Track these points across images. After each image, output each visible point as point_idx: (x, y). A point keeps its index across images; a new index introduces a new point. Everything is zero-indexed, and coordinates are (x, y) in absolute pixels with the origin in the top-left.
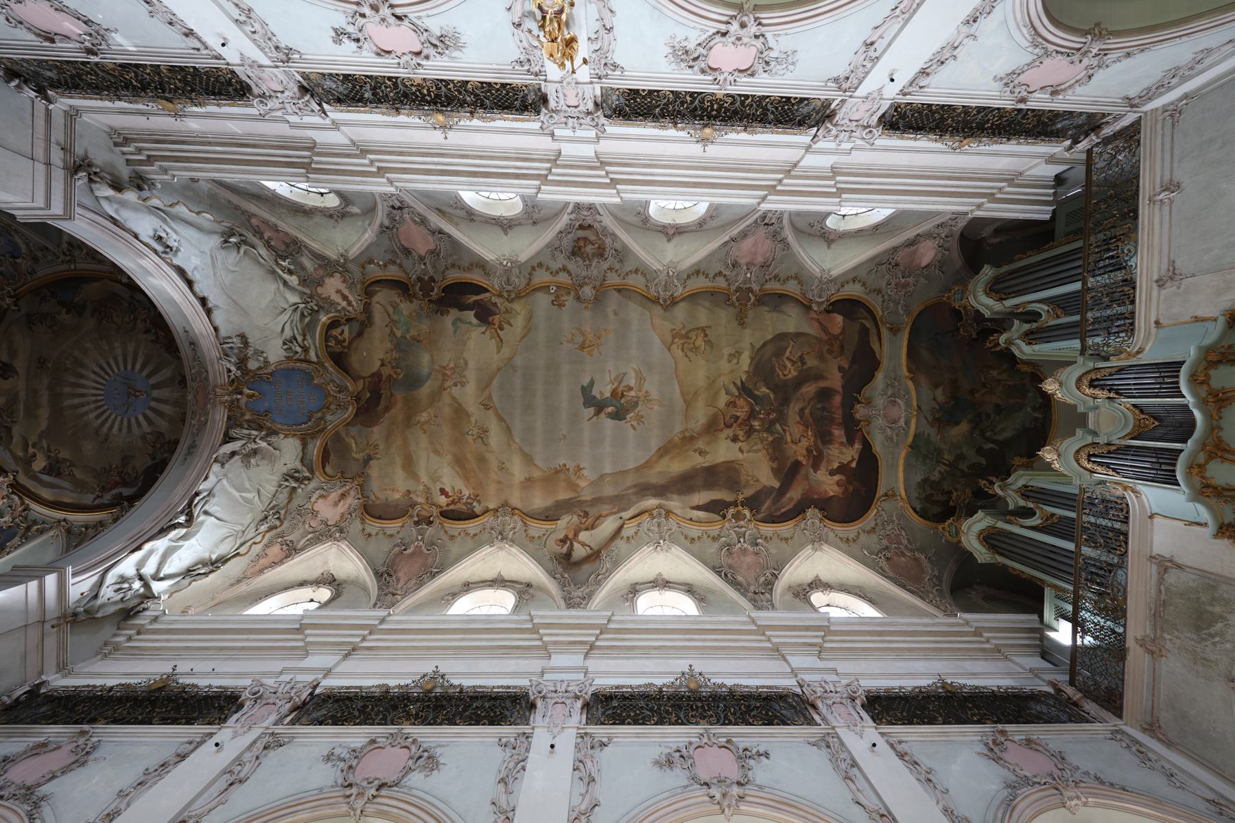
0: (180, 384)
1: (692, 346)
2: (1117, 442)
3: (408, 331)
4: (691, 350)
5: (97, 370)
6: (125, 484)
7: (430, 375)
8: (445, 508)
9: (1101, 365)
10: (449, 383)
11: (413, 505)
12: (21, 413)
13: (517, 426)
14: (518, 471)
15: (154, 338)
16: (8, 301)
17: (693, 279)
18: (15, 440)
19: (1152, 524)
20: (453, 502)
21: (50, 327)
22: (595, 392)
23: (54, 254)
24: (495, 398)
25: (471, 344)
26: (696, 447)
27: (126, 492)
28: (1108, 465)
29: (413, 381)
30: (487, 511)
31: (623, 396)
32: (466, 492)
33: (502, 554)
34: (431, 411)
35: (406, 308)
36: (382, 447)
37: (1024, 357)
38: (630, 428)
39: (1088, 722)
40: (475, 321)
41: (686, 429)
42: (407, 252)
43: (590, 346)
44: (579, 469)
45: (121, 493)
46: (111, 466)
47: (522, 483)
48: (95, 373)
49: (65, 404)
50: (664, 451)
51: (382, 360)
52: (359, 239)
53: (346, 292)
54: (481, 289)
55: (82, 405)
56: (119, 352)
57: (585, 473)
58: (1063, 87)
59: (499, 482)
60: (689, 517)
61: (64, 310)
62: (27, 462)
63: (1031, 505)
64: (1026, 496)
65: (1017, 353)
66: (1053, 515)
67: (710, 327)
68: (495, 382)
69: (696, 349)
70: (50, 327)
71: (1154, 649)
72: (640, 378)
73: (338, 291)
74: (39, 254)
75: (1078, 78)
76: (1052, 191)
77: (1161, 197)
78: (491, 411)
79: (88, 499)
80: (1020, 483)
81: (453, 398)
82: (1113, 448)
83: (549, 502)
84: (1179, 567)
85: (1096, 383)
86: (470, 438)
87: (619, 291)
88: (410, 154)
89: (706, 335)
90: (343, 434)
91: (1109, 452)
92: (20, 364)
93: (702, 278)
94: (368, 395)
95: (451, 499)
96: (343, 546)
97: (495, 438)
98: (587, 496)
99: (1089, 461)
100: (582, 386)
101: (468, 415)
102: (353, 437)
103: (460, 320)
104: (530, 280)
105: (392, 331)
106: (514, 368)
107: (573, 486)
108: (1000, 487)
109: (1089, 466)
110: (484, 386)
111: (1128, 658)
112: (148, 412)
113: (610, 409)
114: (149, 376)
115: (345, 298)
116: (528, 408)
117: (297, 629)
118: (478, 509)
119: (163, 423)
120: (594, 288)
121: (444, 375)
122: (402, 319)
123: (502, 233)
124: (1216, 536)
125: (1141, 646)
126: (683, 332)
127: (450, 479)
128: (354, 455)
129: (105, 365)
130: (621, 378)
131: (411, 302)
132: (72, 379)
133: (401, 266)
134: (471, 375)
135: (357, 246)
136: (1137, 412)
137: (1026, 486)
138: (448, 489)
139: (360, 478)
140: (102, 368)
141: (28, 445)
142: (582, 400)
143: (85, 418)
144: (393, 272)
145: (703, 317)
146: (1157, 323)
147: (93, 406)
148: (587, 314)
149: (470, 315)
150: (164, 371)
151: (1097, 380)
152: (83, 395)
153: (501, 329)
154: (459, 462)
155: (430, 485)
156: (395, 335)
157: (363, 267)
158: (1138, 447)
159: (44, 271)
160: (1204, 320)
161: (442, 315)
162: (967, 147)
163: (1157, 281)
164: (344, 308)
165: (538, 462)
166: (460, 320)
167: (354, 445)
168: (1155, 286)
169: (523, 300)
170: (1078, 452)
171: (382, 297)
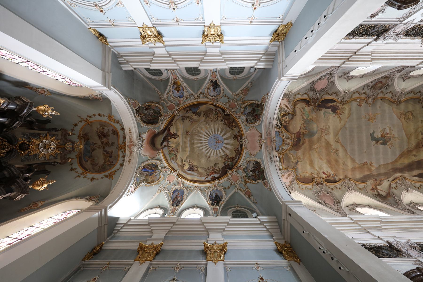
0: (233, 138)
1: (408, 118)
3: (308, 117)
4: (407, 119)
5: (206, 134)
6: (216, 173)
7: (317, 132)
8: (325, 179)
10: (324, 134)
11: (315, 178)
12: (180, 150)
13: (349, 149)
14: (350, 165)
15: (224, 123)
16: (177, 112)
17: (409, 94)
18: (178, 159)
20: (328, 177)
21: (190, 121)
22: (375, 135)
23: (194, 96)
24: (340, 139)
25: (331, 120)
26: (413, 154)
27: (216, 176)
29: (311, 134)
30: (340, 180)
31: (385, 136)
32: (332, 173)
33: (352, 195)
34: (318, 144)
35: (308, 109)
36: (302, 157)
38: (389, 148)
40: (331, 112)
41: (409, 148)
42: (314, 90)
43: (372, 119)
44: (371, 163)
45: (214, 176)
46: (210, 167)
47: (351, 169)
48: (205, 135)
49: (195, 146)
50: (402, 156)
51: (300, 127)
52: (299, 86)
53: (287, 105)
54: (333, 101)
55: (201, 146)
56: (213, 128)
57: (374, 164)
59: (343, 169)
60: (413, 179)
61: (194, 115)
62: (183, 166)
67: (413, 111)
68: (340, 133)
69: (409, 119)
70: (190, 121)
72: (391, 130)
73: (284, 104)
74: (189, 96)
78: (339, 144)
79: (203, 179)
81: (326, 140)
83: (362, 176)
86: (332, 153)
87: (381, 99)
88: (386, 53)
89: (412, 114)
90: (288, 154)
92: (180, 133)
93: (412, 94)
94: (296, 139)
95: (327, 175)
96: (296, 193)
97: (341, 153)
98: (375, 173)
100: (371, 134)
101: (331, 145)
102: (292, 155)
103: (326, 112)
104: (351, 97)
105: (303, 117)
106: (346, 128)
107: (370, 170)
110: (336, 135)
112: (223, 148)
113: (381, 141)
114: (223, 136)
115: (287, 107)
116: (352, 142)
117: (354, 222)
118: (337, 179)
119: (228, 151)
120: (373, 99)
121: (322, 131)
122: (306, 113)
123: (347, 81)
126: (404, 113)
127: (326, 168)
128: (292, 161)
129: (208, 133)
130: (384, 130)
131: (309, 107)
132: (197, 138)
133: (308, 95)
134: (331, 131)
135: (297, 89)
138: (325, 172)
139: (295, 168)
140: (207, 133)
141: (183, 161)
142: (371, 139)
143: (202, 151)
144: (305, 97)
145: (410, 108)
147: (204, 147)
148: (370, 108)
149: (329, 110)
150: (228, 134)
152: (201, 143)
153: (341, 114)
154: (329, 162)
155: (319, 171)
156: (304, 119)
157: (295, 96)
159: (189, 102)
161: (320, 110)
164: (287, 110)
165: (357, 161)
166: (326, 112)
167: (292, 157)
169: (348, 104)
171: (299, 105)
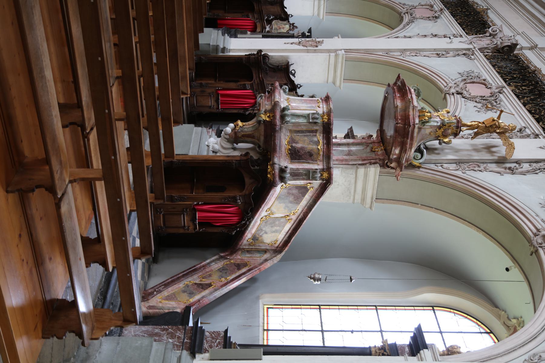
162: (484, 7)
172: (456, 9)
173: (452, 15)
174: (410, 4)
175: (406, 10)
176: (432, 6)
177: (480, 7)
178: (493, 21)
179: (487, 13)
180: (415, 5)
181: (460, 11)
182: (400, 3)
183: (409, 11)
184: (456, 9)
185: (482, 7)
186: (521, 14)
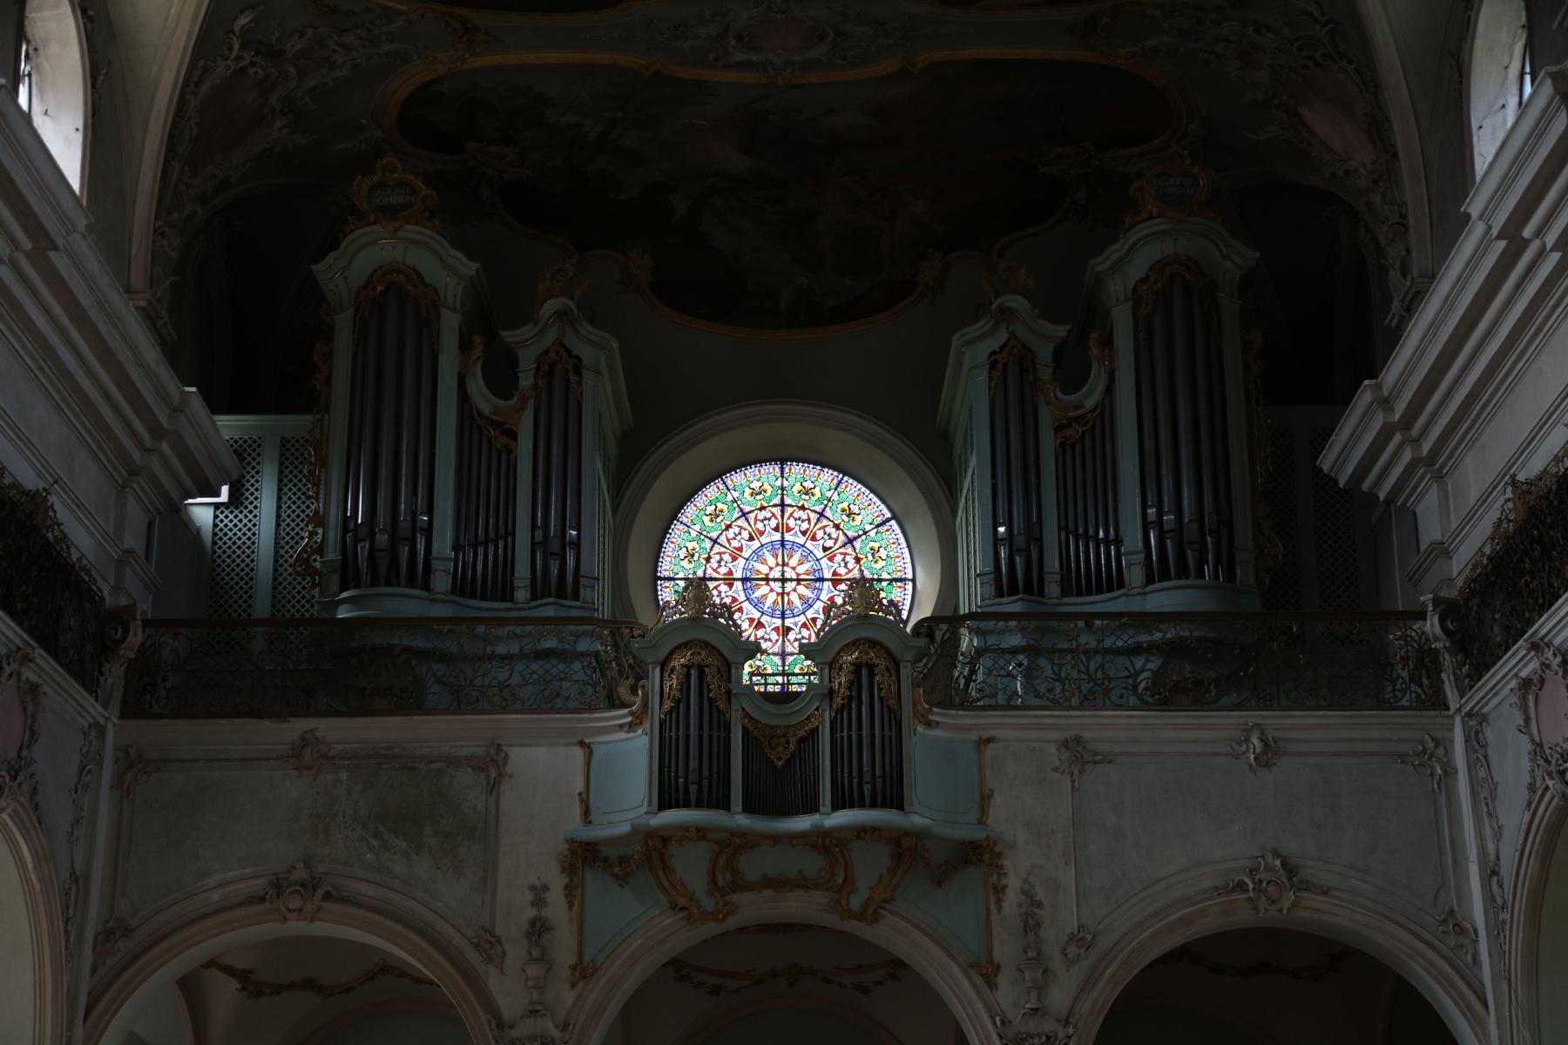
2: (735, 705)
9: (906, 671)
19: (567, 745)
28: (682, 700)
37: (955, 340)
39: (91, 692)
58: (1531, 698)
63: (526, 381)
64: (546, 368)
65: (973, 331)
66: (513, 435)
71: (299, 755)
75: (1534, 723)
76: (1382, 495)
77: (1255, 741)
80: (581, 349)
82: (721, 704)
84: (493, 788)
85: (864, 672)
91: (711, 700)
99: (688, 667)
108: (562, 316)
109: (679, 661)
111: (266, 723)
124: (571, 841)
125: (303, 739)
136: (801, 734)
137: (577, 370)
146: (989, 740)
151: (871, 675)
158: (728, 740)
160: (983, 810)
162: (1509, 494)
163: (1078, 740)
168: (1067, 734)
170: (706, 645)
172: (1525, 594)
173: (1551, 605)
174: (1526, 765)
175: (1552, 778)
176: (1526, 684)
177: (1510, 510)
178: (1556, 456)
179: (1530, 483)
180: (1529, 747)
181: (1533, 579)
182: (1530, 803)
183: (1553, 768)
184: (1525, 594)
185: (1510, 505)
186: (1521, 364)
